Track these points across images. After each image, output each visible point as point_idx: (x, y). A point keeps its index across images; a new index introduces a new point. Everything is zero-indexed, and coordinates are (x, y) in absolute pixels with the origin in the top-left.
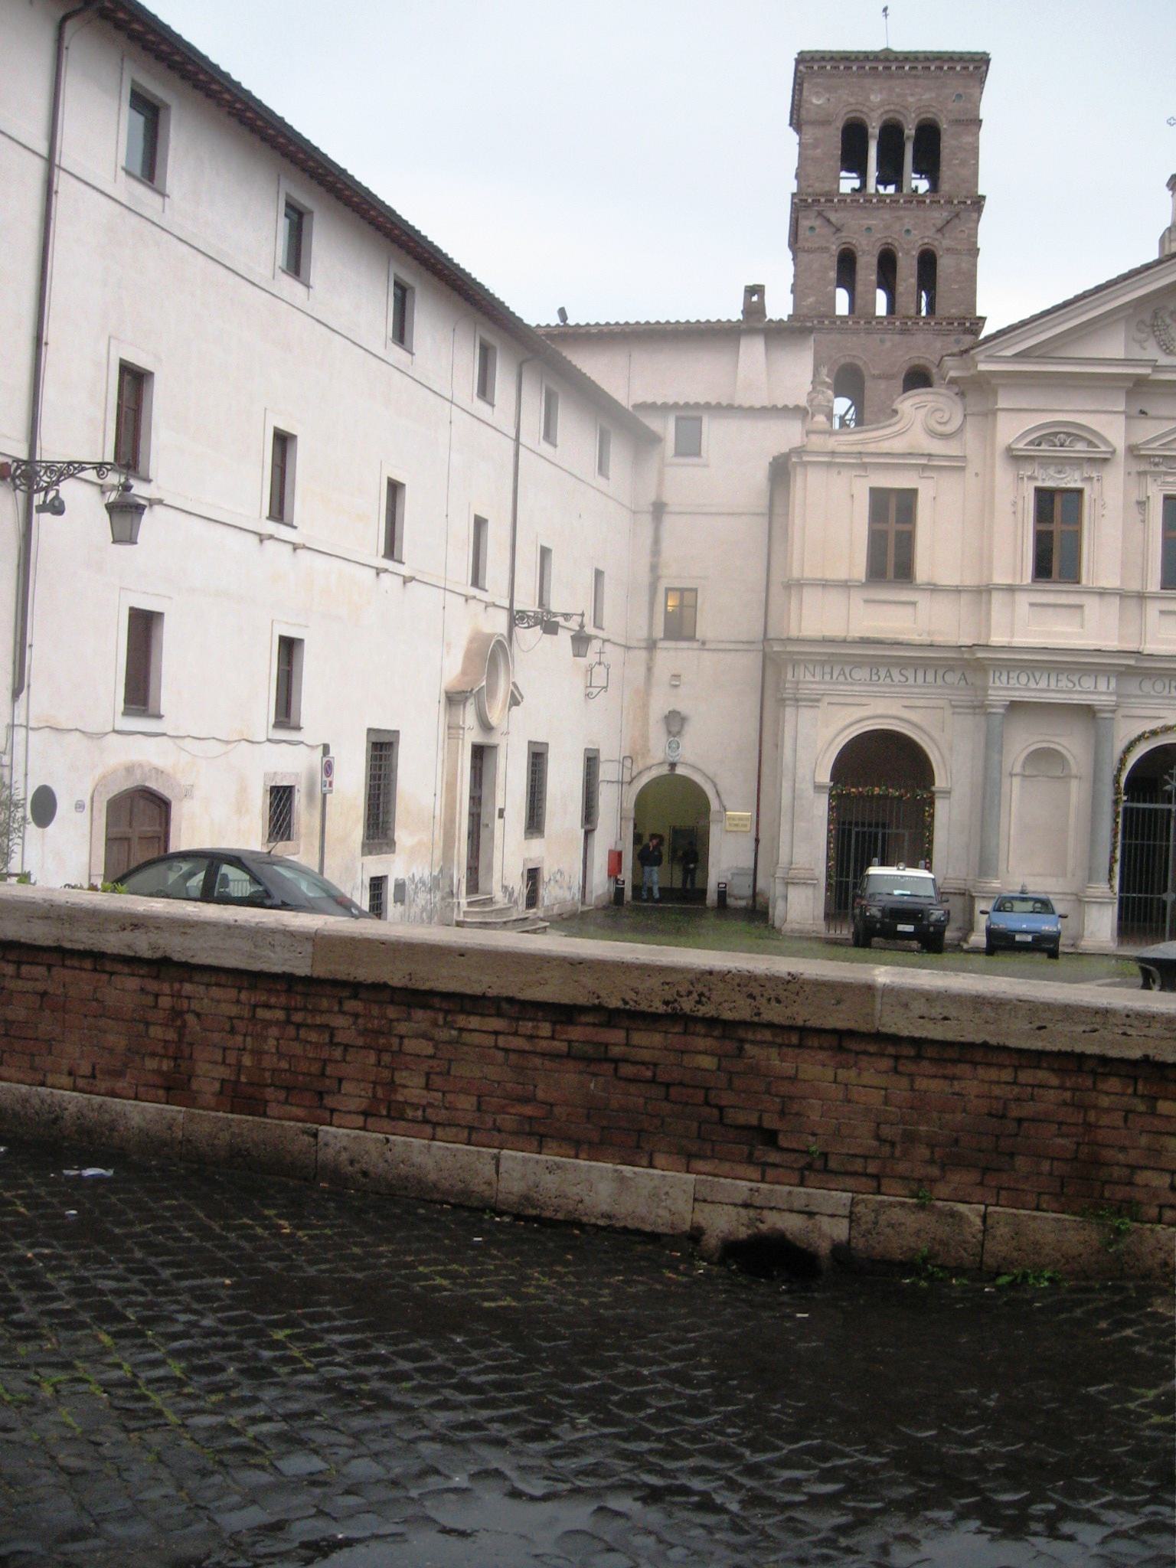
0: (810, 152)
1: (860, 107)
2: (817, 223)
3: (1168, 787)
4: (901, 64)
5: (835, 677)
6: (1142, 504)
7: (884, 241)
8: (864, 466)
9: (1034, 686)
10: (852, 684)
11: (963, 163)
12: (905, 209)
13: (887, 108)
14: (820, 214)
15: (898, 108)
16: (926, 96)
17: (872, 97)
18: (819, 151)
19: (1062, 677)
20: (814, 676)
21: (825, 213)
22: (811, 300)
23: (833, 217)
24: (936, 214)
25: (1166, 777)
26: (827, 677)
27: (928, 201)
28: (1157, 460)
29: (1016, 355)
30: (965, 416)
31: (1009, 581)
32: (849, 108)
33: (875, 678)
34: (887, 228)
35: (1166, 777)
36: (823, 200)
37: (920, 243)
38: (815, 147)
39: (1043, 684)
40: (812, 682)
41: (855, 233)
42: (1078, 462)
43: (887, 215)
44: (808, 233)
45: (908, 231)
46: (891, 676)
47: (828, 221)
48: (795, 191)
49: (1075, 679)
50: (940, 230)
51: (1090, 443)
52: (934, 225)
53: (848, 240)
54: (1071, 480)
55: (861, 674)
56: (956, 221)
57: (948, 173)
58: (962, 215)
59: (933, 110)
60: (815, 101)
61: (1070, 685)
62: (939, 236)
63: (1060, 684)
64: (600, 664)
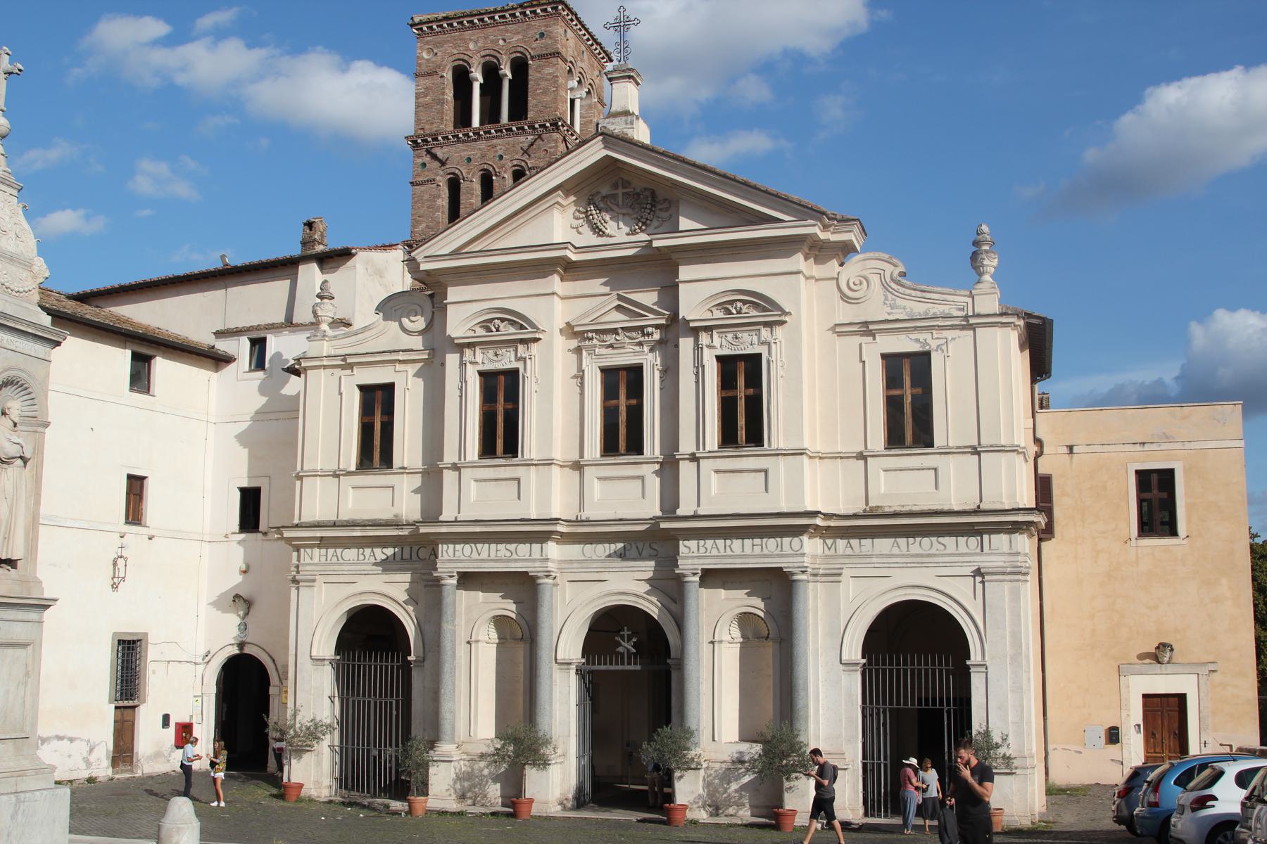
0: (421, 100)
1: (461, 56)
2: (427, 159)
3: (620, 649)
4: (492, 15)
5: (329, 559)
6: (580, 377)
7: (481, 167)
8: (351, 366)
9: (477, 557)
10: (341, 564)
11: (546, 91)
12: (497, 138)
13: (483, 53)
14: (429, 152)
15: (492, 52)
16: (515, 39)
17: (471, 46)
18: (429, 98)
19: (502, 547)
20: (311, 559)
21: (433, 151)
22: (423, 225)
23: (439, 153)
24: (522, 139)
25: (618, 639)
26: (323, 559)
27: (514, 128)
28: (590, 335)
29: (451, 254)
30: (433, 313)
31: (456, 460)
32: (454, 58)
33: (361, 557)
34: (483, 156)
35: (618, 639)
36: (430, 139)
37: (510, 165)
38: (426, 96)
39: (484, 555)
40: (310, 564)
41: (458, 164)
42: (513, 343)
43: (483, 145)
44: (420, 170)
45: (501, 157)
46: (374, 555)
47: (434, 157)
48: (412, 133)
49: (512, 547)
50: (525, 152)
51: (522, 327)
52: (522, 148)
53: (452, 171)
54: (506, 360)
55: (350, 554)
56: (539, 142)
57: (534, 102)
58: (544, 136)
59: (520, 49)
60: (425, 56)
61: (509, 554)
62: (525, 157)
63: (499, 554)
64: (121, 557)
